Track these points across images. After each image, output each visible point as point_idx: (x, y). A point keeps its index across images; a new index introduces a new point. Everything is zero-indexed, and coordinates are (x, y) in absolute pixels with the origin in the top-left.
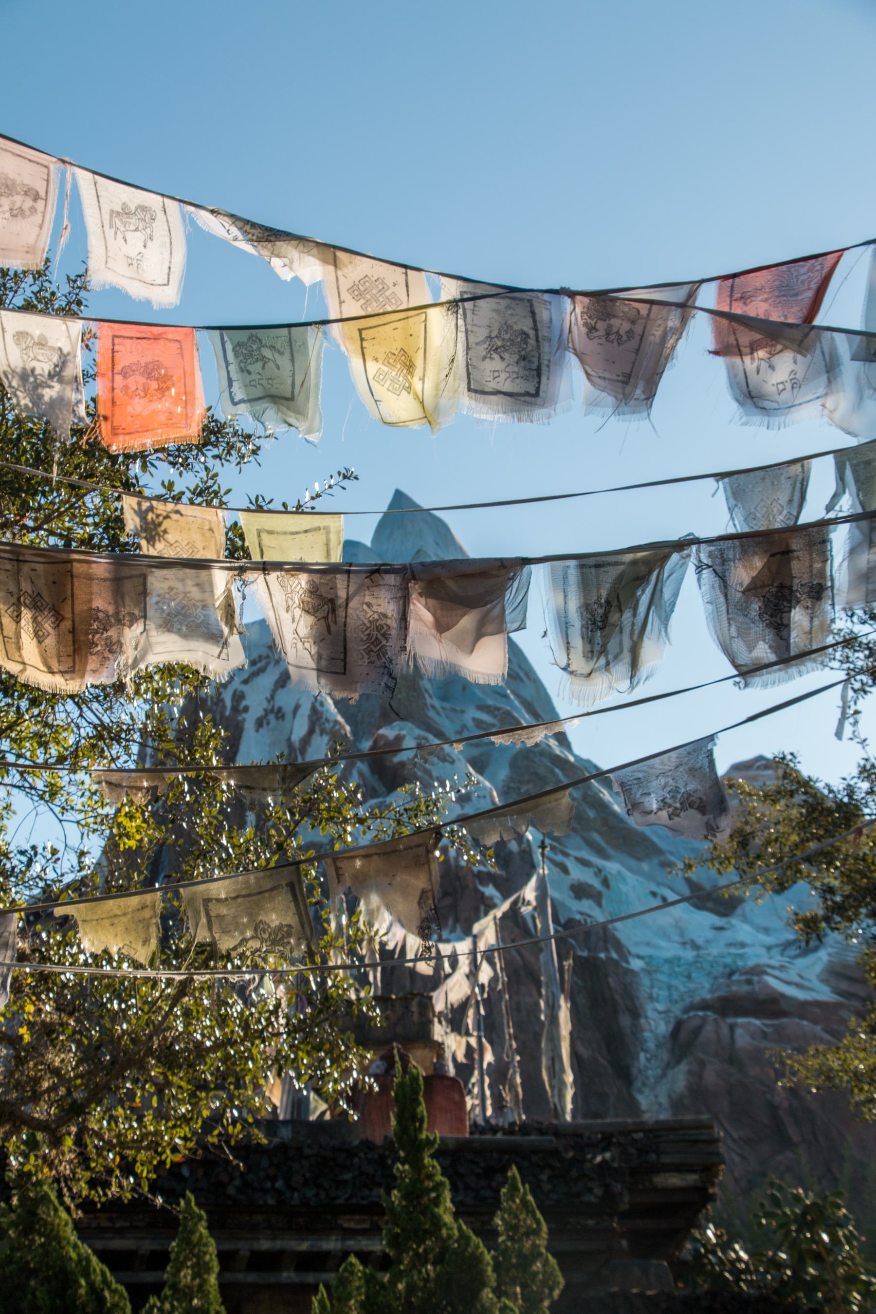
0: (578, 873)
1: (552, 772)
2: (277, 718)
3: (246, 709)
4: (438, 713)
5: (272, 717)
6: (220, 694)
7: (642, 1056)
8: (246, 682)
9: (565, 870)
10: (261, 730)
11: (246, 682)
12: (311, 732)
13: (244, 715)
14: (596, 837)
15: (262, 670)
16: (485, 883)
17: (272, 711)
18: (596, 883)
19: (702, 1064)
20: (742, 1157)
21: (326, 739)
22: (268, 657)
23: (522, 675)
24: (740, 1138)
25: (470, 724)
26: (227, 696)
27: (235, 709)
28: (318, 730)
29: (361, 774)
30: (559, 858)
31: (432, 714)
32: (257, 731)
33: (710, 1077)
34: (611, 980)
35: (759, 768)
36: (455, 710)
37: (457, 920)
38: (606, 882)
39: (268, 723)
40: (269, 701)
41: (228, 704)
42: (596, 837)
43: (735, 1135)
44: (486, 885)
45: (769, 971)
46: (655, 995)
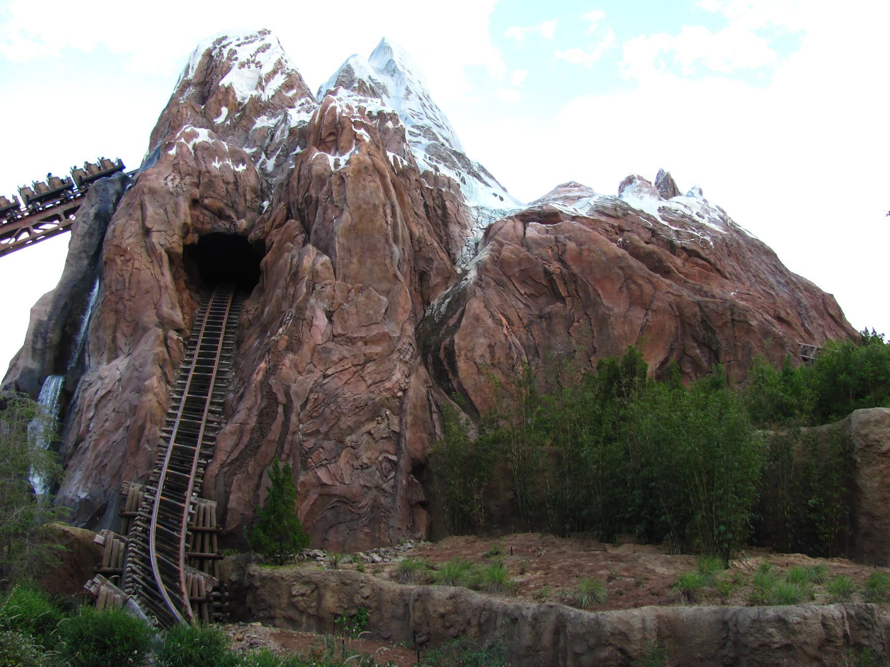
1: (450, 156)
2: (257, 67)
3: (236, 59)
5: (253, 66)
7: (465, 248)
8: (239, 45)
10: (242, 69)
11: (239, 45)
12: (275, 72)
13: (234, 62)
17: (253, 62)
19: (501, 245)
20: (527, 306)
21: (284, 76)
22: (256, 36)
24: (525, 293)
26: (225, 52)
27: (229, 59)
28: (280, 72)
30: (434, 163)
32: (240, 68)
33: (506, 253)
34: (447, 203)
35: (571, 187)
37: (337, 149)
39: (249, 67)
40: (252, 56)
41: (225, 55)
43: (522, 292)
44: (360, 129)
46: (479, 220)
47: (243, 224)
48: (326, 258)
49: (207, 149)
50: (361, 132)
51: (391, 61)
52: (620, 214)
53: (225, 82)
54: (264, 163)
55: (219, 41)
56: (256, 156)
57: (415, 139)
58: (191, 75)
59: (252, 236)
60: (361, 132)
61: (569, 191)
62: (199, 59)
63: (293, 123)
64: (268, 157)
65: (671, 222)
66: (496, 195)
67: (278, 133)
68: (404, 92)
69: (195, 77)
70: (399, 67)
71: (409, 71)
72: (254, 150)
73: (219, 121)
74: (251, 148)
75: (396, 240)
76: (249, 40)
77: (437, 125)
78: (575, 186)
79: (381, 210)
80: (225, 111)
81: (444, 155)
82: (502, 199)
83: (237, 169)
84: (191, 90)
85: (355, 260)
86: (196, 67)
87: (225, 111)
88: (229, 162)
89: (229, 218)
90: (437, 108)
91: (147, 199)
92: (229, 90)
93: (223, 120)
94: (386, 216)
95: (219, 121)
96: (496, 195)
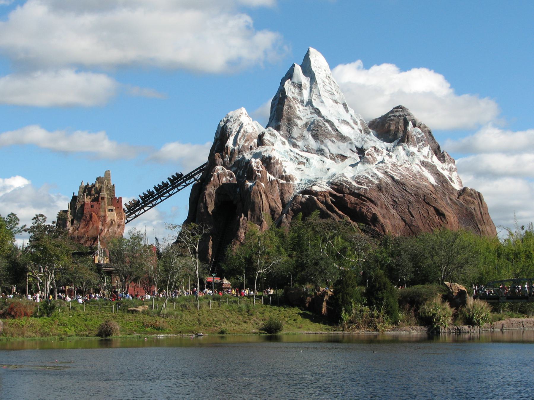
0: (300, 159)
1: (324, 124)
4: (300, 112)
6: (226, 129)
8: (231, 126)
12: (242, 136)
14: (334, 139)
15: (235, 123)
16: (258, 172)
18: (305, 161)
23: (335, 93)
25: (309, 113)
29: (254, 143)
31: (298, 113)
36: (306, 109)
42: (334, 139)
45: (317, 184)
48: (246, 218)
49: (222, 175)
50: (259, 174)
52: (338, 184)
54: (239, 173)
57: (312, 116)
58: (218, 136)
59: (235, 203)
60: (259, 174)
61: (397, 111)
63: (246, 161)
64: (240, 171)
65: (358, 183)
66: (321, 160)
67: (243, 162)
69: (219, 137)
70: (314, 69)
71: (319, 68)
72: (236, 168)
74: (236, 167)
75: (263, 211)
77: (331, 94)
78: (401, 108)
79: (259, 203)
81: (321, 124)
82: (323, 162)
84: (219, 142)
85: (253, 217)
86: (219, 133)
88: (228, 178)
90: (333, 81)
91: (207, 197)
92: (227, 147)
93: (227, 159)
94: (260, 204)
96: (321, 160)
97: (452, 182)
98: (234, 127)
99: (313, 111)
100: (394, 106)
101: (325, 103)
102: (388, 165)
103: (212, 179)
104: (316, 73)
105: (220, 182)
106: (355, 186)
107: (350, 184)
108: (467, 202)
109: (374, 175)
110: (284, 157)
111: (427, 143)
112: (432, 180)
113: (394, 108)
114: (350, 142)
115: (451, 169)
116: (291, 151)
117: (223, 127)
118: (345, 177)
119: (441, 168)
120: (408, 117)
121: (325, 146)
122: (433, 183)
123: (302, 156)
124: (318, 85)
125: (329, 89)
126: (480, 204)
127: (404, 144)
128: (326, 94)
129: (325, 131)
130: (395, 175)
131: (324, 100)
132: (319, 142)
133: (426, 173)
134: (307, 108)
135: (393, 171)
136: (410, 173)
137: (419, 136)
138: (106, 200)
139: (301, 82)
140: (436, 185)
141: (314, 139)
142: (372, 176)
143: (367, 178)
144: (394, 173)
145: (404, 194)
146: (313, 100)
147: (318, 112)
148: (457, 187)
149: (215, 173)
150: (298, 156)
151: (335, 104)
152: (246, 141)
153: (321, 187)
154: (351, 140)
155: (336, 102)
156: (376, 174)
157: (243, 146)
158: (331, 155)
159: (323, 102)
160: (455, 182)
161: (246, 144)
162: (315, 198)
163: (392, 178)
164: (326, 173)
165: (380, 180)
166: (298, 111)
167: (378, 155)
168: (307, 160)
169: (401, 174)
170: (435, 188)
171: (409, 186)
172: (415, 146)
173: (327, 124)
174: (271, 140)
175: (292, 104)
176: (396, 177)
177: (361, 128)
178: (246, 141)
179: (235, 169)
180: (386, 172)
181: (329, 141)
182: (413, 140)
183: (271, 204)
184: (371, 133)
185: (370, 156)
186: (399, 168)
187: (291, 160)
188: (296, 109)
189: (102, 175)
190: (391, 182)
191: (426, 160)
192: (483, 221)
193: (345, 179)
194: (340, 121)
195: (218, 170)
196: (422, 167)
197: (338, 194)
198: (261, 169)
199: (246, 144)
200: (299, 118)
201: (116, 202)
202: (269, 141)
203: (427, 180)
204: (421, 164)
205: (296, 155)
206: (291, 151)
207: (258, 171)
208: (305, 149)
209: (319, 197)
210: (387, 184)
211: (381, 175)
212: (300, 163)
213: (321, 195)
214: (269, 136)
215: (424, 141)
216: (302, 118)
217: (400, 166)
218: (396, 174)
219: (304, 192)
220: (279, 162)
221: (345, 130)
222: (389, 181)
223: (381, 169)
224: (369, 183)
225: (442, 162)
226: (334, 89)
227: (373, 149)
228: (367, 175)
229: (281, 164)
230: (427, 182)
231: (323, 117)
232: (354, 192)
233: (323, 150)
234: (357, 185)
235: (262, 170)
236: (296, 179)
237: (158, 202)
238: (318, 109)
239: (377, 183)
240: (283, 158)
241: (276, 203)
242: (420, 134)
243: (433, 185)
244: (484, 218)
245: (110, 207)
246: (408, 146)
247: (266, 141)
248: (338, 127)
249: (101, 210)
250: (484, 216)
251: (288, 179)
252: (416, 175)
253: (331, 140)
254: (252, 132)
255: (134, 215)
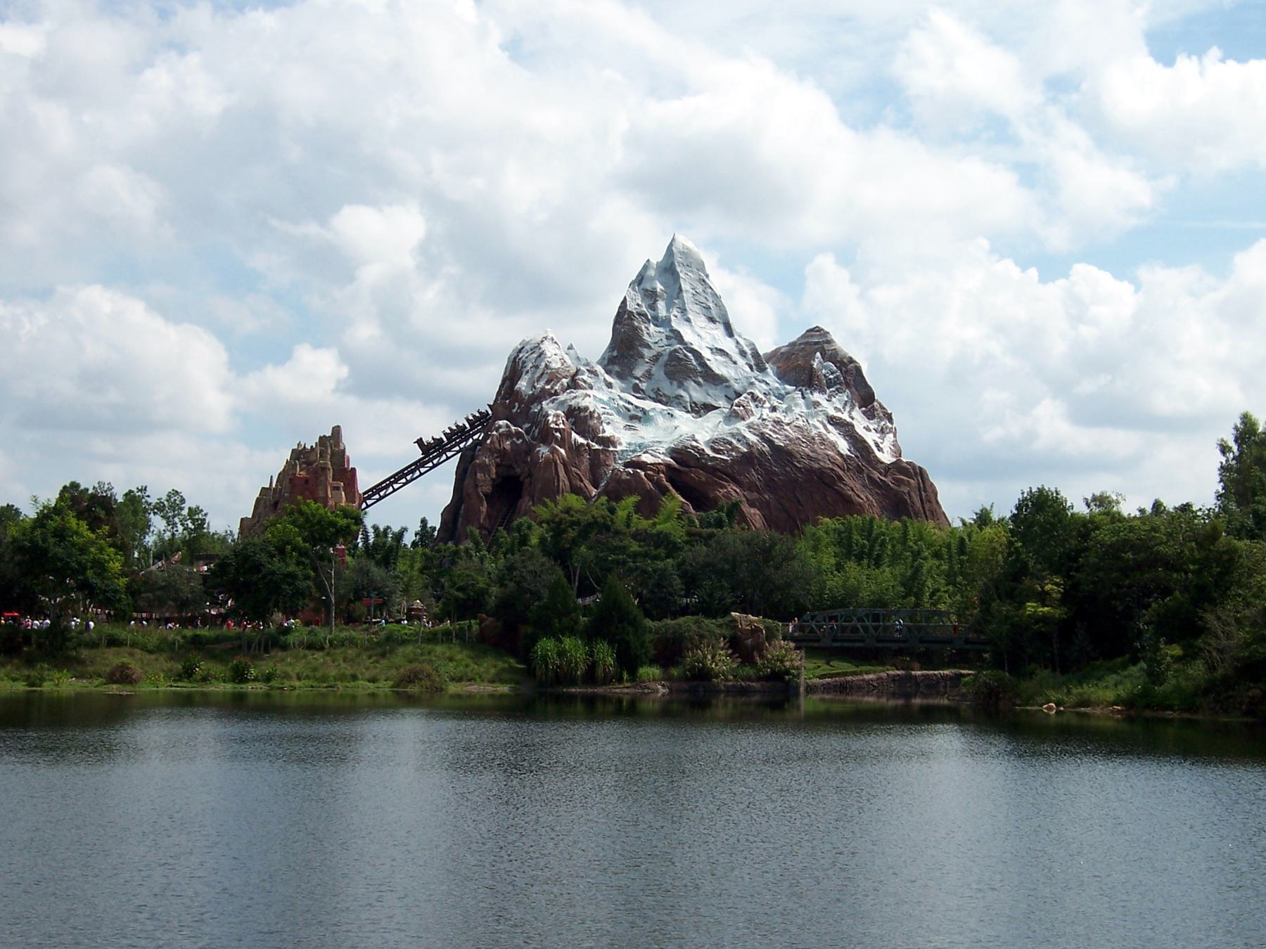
1: (686, 356)
9: (629, 410)
18: (640, 414)
31: (646, 337)
38: (645, 413)
42: (700, 380)
45: (650, 451)
47: (518, 470)
50: (558, 434)
51: (673, 263)
53: (517, 386)
55: (520, 351)
56: (531, 427)
58: (507, 374)
59: (521, 479)
60: (558, 434)
61: (812, 336)
62: (510, 364)
68: (677, 290)
70: (679, 269)
73: (514, 411)
76: (533, 350)
78: (818, 331)
80: (517, 404)
83: (518, 442)
84: (508, 383)
87: (517, 404)
89: (514, 468)
90: (711, 288)
92: (519, 392)
95: (514, 411)
97: (879, 450)
98: (530, 360)
99: (672, 335)
100: (808, 328)
101: (693, 324)
102: (767, 423)
103: (489, 441)
104: (681, 275)
105: (500, 445)
106: (708, 455)
107: (701, 452)
108: (899, 482)
109: (742, 439)
110: (608, 407)
111: (844, 387)
112: (844, 446)
113: (808, 331)
114: (725, 384)
115: (884, 430)
116: (621, 398)
117: (515, 358)
118: (696, 441)
119: (864, 428)
120: (826, 346)
121: (684, 390)
122: (842, 452)
123: (637, 407)
124: (685, 294)
125: (704, 301)
126: (922, 485)
127: (804, 389)
128: (696, 308)
129: (686, 367)
130: (777, 438)
131: (690, 316)
132: (675, 383)
133: (834, 436)
134: (661, 329)
135: (774, 432)
136: (804, 436)
137: (831, 377)
138: (330, 474)
139: (656, 288)
140: (848, 456)
141: (669, 378)
142: (739, 440)
143: (731, 444)
144: (774, 436)
145: (788, 469)
146: (673, 318)
147: (678, 336)
148: (886, 457)
149: (494, 433)
150: (630, 407)
151: (712, 325)
152: (548, 383)
153: (655, 456)
154: (727, 381)
155: (712, 320)
156: (745, 437)
157: (543, 389)
158: (693, 405)
159: (688, 320)
160: (885, 451)
161: (548, 387)
162: (643, 473)
163: (769, 442)
164: (671, 433)
165: (748, 445)
166: (646, 335)
167: (757, 406)
168: (645, 413)
169: (786, 436)
170: (845, 460)
171: (798, 456)
172: (822, 391)
173: (689, 355)
174: (589, 380)
175: (636, 324)
176: (777, 442)
177: (752, 363)
178: (548, 383)
179: (527, 426)
180: (762, 434)
181: (693, 383)
182: (820, 382)
183: (574, 482)
184: (769, 370)
185: (742, 408)
186: (786, 427)
187: (619, 413)
188: (642, 331)
189: (329, 434)
190: (768, 449)
191: (839, 415)
192: (925, 513)
193: (694, 444)
194: (714, 351)
195: (500, 427)
196: (830, 427)
197: (682, 468)
198: (562, 426)
199: (548, 387)
200: (648, 347)
201: (348, 477)
202: (585, 382)
203: (833, 446)
204: (829, 422)
205: (627, 405)
206: (621, 398)
207: (557, 430)
208: (653, 395)
209: (649, 472)
210: (762, 453)
211: (753, 438)
212: (633, 418)
213: (651, 469)
214: (587, 373)
215: (840, 384)
216: (652, 346)
217: (788, 424)
218: (779, 436)
219: (627, 465)
220: (596, 415)
221: (718, 365)
222: (766, 448)
223: (755, 429)
224: (732, 450)
225: (869, 419)
226: (710, 300)
227: (749, 397)
228: (729, 439)
229: (599, 417)
230: (833, 451)
231: (686, 344)
232: (706, 464)
233: (682, 396)
234: (712, 454)
235: (563, 429)
236: (620, 444)
237: (415, 476)
238: (679, 332)
239: (745, 450)
240: (605, 408)
241: (582, 481)
242: (832, 374)
243: (841, 455)
244: (927, 508)
245: (335, 484)
246: (811, 393)
247: (581, 383)
248: (709, 360)
249: (320, 488)
250: (927, 506)
251: (608, 442)
252: (814, 439)
253: (695, 382)
254: (559, 368)
255: (377, 496)
